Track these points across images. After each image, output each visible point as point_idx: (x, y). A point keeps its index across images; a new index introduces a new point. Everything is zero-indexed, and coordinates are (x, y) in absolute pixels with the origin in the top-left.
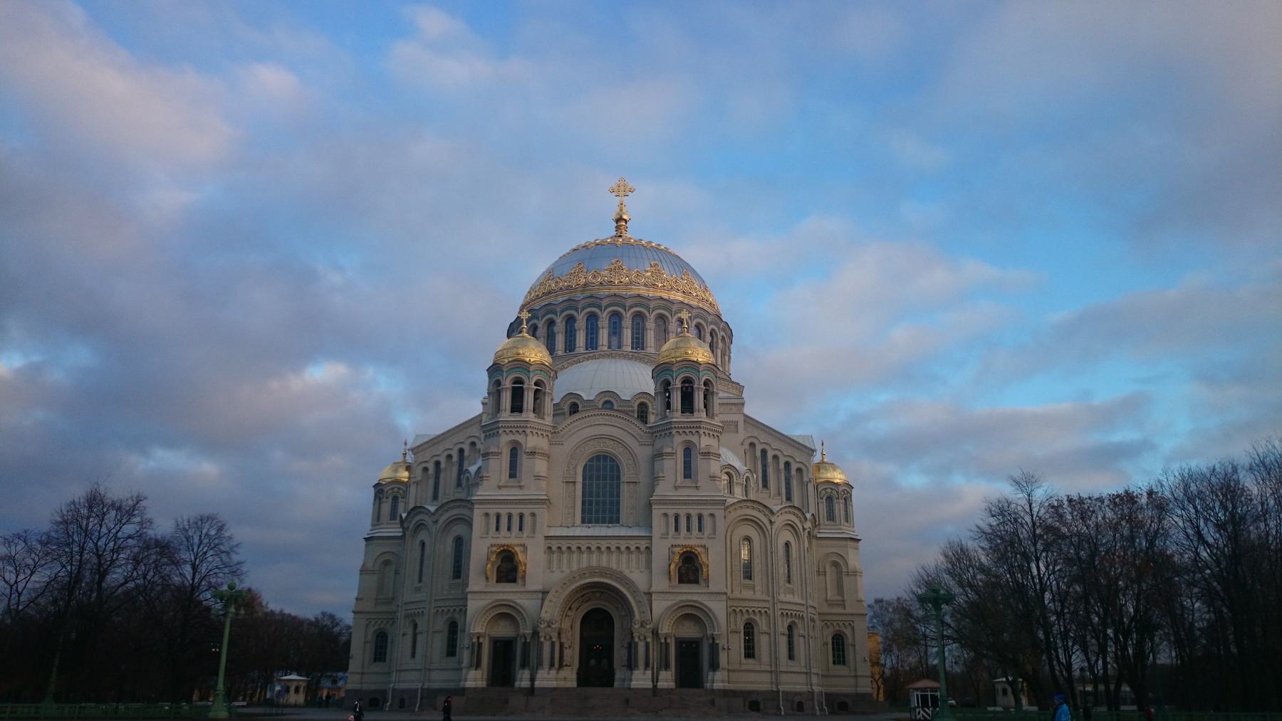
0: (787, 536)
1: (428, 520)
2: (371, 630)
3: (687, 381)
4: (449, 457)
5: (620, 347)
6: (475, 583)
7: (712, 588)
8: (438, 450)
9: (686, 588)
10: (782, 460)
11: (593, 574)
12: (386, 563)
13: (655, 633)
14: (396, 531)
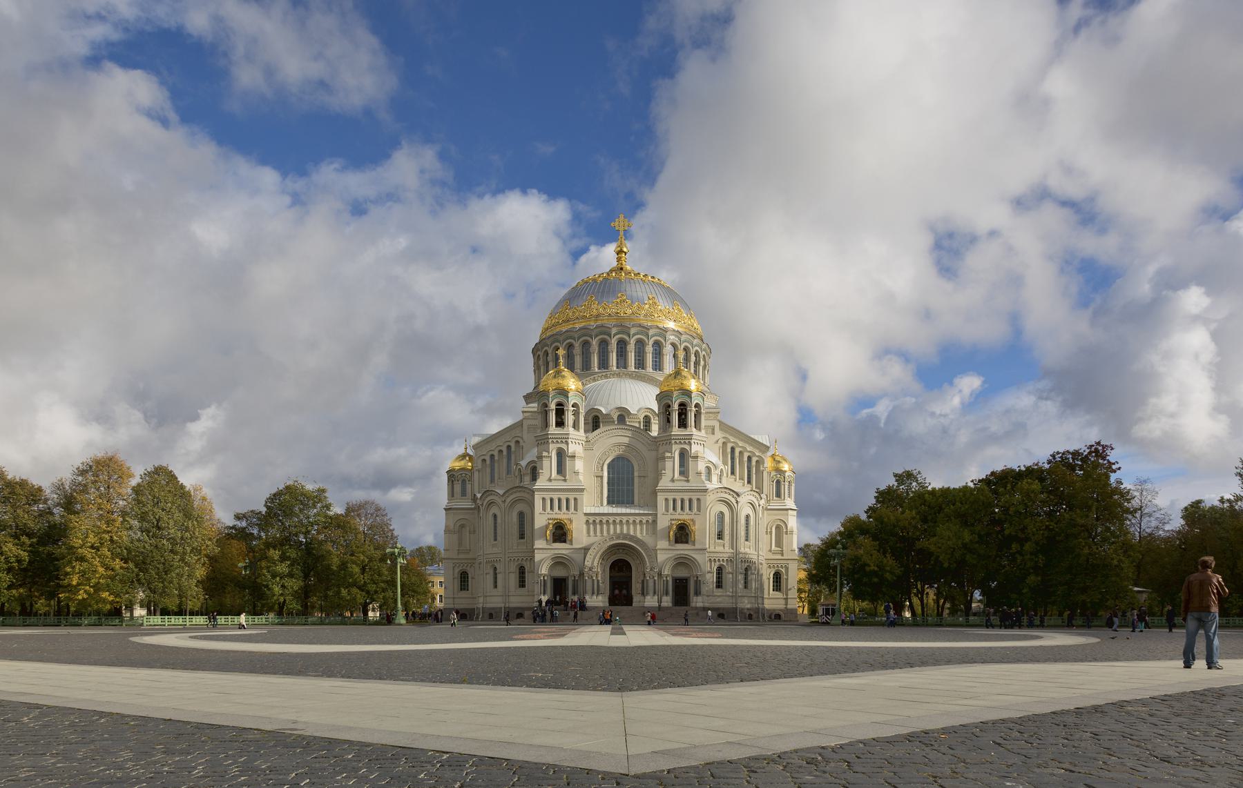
0: (749, 511)
1: (499, 500)
2: (457, 570)
3: (682, 405)
4: (501, 451)
5: (625, 367)
6: (539, 544)
7: (697, 546)
8: (493, 446)
9: (680, 546)
10: (746, 455)
11: (618, 538)
12: (462, 526)
13: (660, 575)
14: (468, 504)
